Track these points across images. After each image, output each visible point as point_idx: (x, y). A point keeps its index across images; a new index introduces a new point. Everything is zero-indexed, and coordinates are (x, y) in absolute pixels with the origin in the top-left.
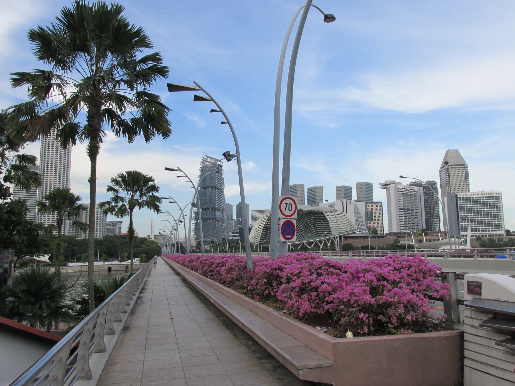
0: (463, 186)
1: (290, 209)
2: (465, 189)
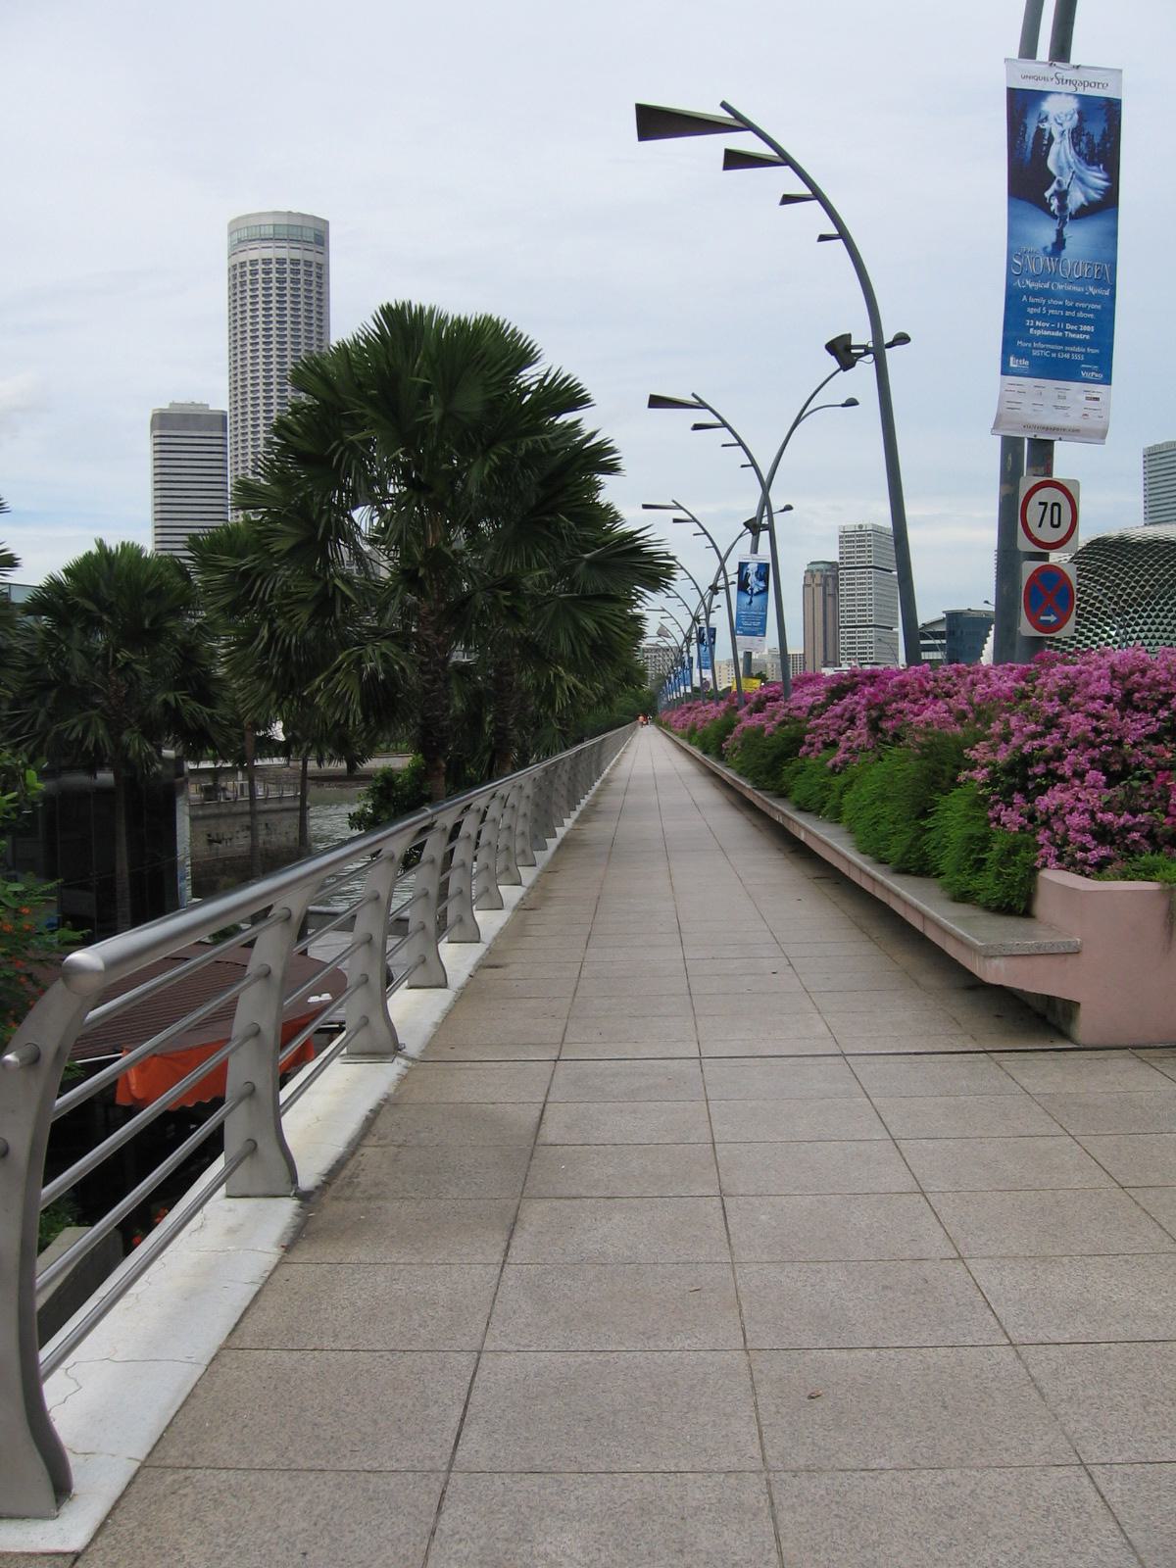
1: (1056, 522)
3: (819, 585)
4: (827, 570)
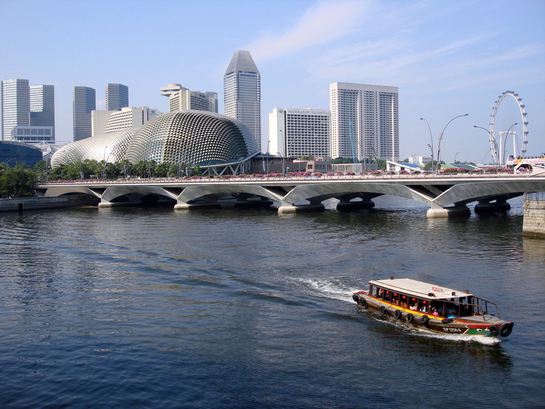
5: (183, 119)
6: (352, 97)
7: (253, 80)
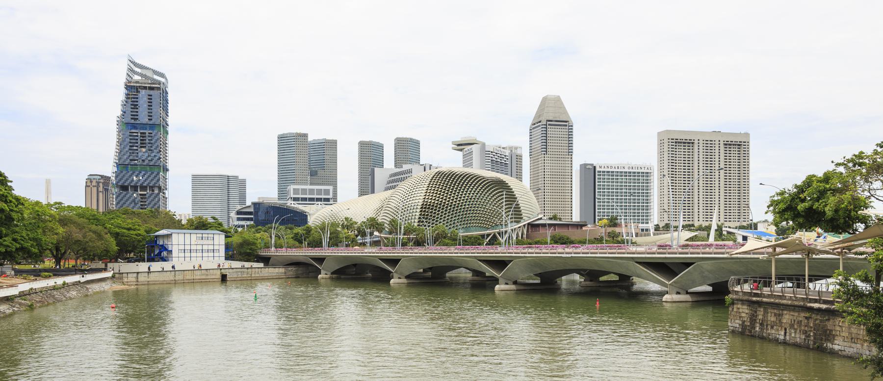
0: (564, 154)
2: (566, 159)
3: (95, 186)
4: (99, 179)
5: (443, 178)
6: (687, 148)
7: (564, 130)
